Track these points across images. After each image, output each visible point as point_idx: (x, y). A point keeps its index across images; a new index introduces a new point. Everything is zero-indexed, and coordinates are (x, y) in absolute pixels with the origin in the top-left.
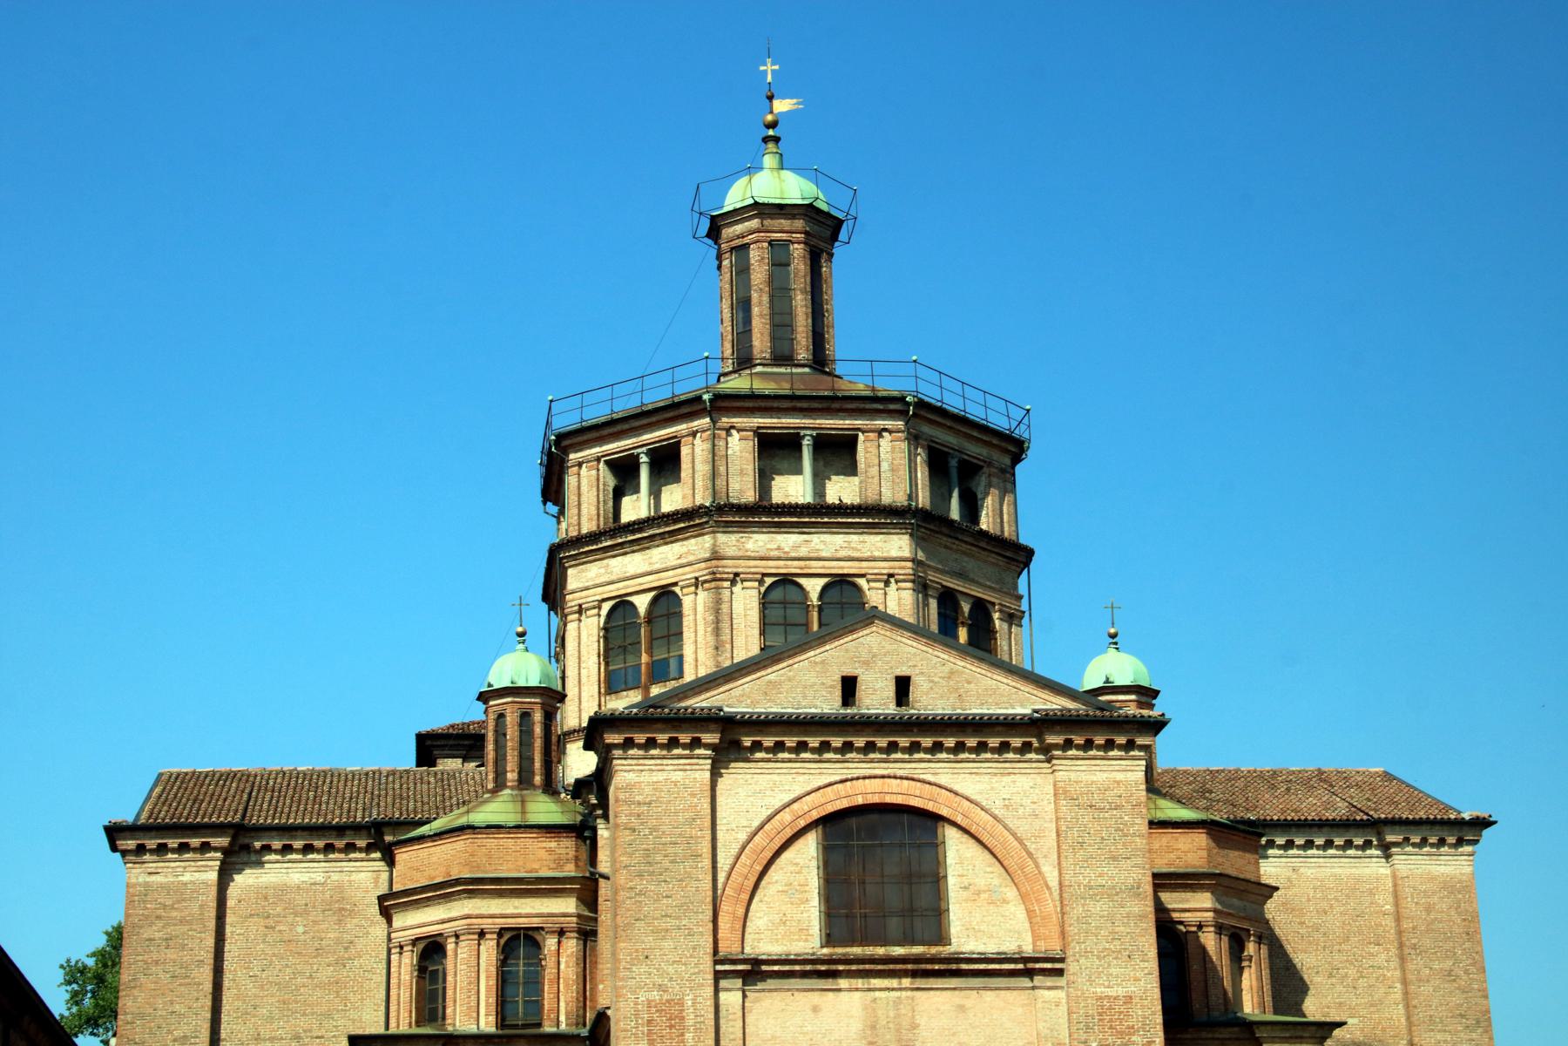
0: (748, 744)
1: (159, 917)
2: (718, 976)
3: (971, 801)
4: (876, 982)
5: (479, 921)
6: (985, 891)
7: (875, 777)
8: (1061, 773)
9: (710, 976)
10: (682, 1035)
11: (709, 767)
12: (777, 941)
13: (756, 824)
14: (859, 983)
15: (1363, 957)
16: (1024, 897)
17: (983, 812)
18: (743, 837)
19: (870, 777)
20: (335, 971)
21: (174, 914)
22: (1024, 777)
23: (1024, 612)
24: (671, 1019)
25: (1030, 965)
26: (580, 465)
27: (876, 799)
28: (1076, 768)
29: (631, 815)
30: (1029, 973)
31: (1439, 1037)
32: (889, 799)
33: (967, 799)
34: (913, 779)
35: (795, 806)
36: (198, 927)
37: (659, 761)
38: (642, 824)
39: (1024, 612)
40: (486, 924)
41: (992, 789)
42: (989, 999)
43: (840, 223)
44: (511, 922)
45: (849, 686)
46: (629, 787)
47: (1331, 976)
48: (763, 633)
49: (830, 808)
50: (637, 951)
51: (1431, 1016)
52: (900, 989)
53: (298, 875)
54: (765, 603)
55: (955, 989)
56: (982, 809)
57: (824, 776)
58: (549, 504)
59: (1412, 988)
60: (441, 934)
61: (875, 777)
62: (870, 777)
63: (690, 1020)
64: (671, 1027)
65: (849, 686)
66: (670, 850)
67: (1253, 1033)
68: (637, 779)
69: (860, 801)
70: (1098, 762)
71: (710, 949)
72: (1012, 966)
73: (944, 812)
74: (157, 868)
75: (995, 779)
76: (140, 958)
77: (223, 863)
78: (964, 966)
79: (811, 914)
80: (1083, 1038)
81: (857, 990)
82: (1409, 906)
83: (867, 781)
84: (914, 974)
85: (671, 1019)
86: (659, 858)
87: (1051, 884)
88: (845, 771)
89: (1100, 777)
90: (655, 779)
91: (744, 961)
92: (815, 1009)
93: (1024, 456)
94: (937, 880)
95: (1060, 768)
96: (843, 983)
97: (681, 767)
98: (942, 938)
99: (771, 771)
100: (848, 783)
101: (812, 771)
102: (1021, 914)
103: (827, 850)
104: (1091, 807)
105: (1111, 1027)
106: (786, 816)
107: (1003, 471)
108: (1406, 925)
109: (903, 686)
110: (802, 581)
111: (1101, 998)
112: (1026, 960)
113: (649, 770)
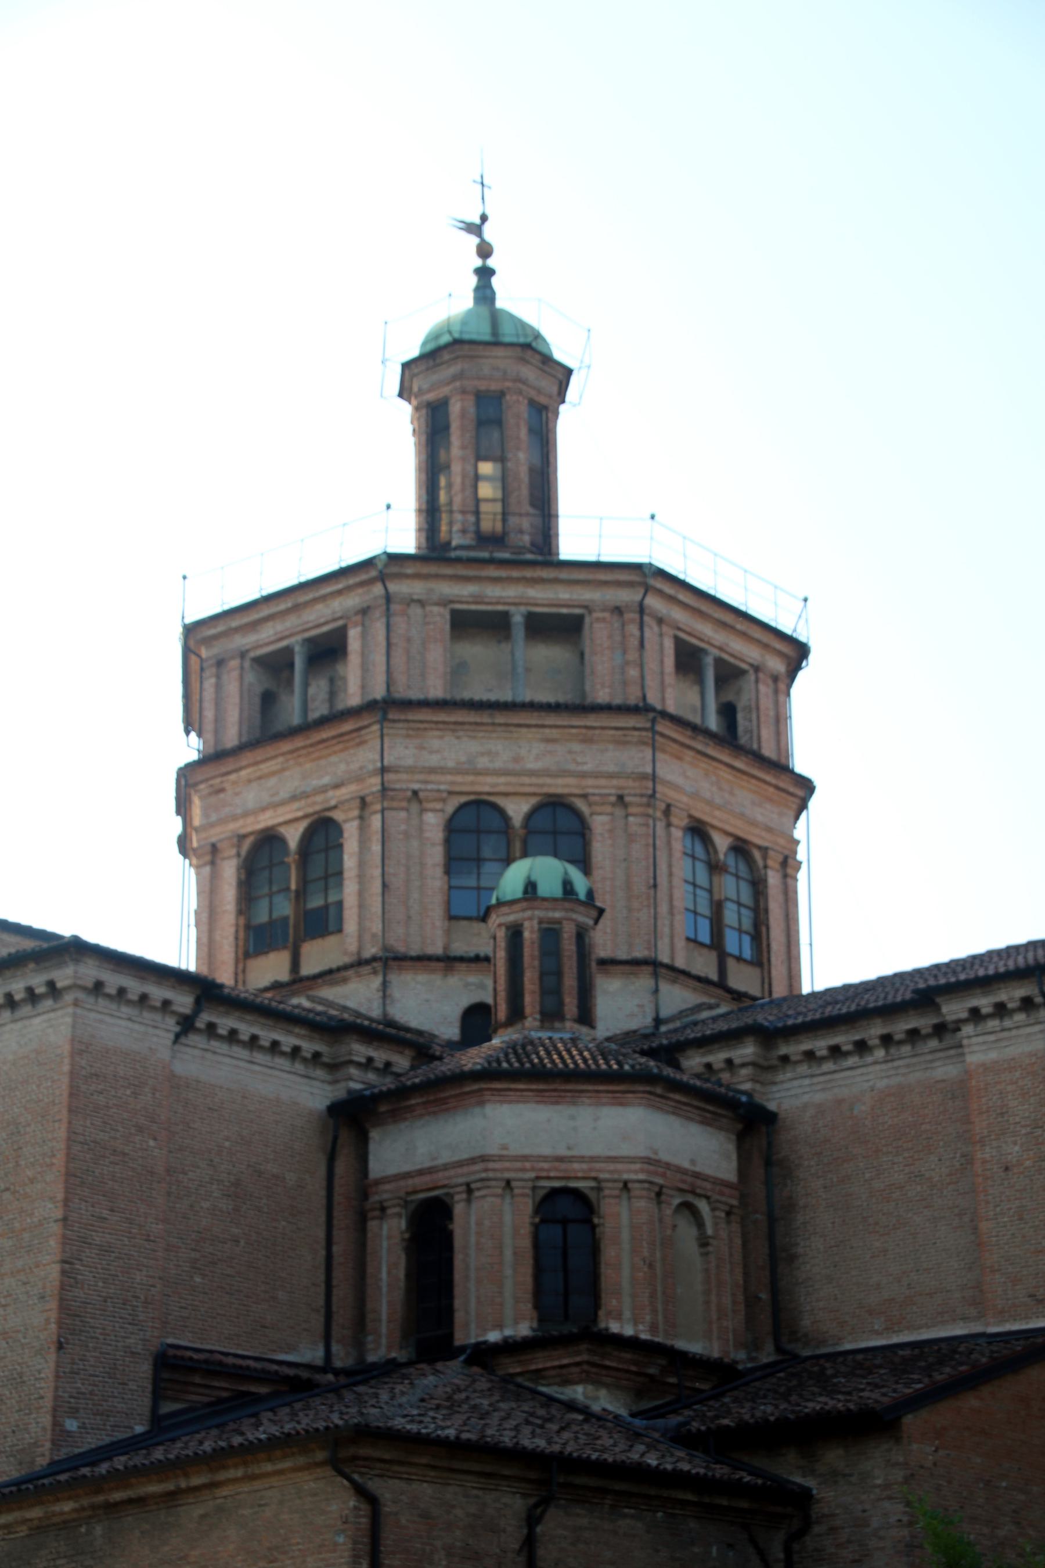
23: (800, 863)
39: (800, 863)
43: (569, 372)
48: (448, 871)
54: (452, 829)
58: (193, 735)
93: (804, 664)
107: (775, 679)
110: (500, 801)
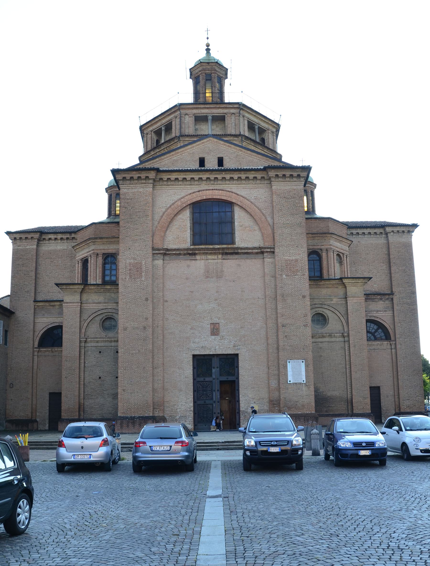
0: (166, 179)
1: (21, 258)
2: (153, 254)
3: (243, 197)
4: (209, 257)
5: (97, 251)
6: (248, 227)
7: (210, 190)
8: (274, 187)
9: (151, 255)
10: (141, 274)
11: (152, 186)
12: (175, 244)
13: (168, 206)
14: (203, 257)
15: (379, 267)
16: (260, 229)
17: (247, 201)
18: (164, 210)
19: (208, 190)
20: (70, 274)
21: (25, 257)
22: (262, 189)
24: (137, 269)
25: (263, 250)
26: (147, 134)
27: (210, 197)
28: (280, 185)
29: (125, 203)
30: (262, 253)
31: (401, 289)
32: (214, 197)
33: (242, 196)
34: (223, 190)
35: (182, 200)
36: (31, 261)
37: (135, 185)
38: (129, 206)
40: (99, 252)
41: (251, 193)
42: (248, 262)
44: (106, 252)
45: (202, 162)
46: (125, 194)
47: (369, 272)
49: (194, 200)
50: (126, 247)
51: (398, 283)
52: (218, 259)
53: (59, 247)
55: (237, 259)
56: (247, 200)
57: (192, 190)
59: (393, 275)
60: (87, 256)
61: (210, 190)
62: (208, 190)
63: (144, 269)
64: (137, 271)
65: (202, 162)
66: (138, 214)
67: (342, 281)
68: (127, 191)
69: (205, 198)
70: (287, 183)
71: (151, 245)
72: (257, 251)
73: (234, 201)
74: (20, 244)
75: (252, 190)
76: (16, 269)
77: (38, 243)
78: (240, 251)
79: (187, 235)
80: (280, 274)
81: (203, 259)
82: (392, 251)
83: (207, 191)
84: (222, 254)
85: (137, 269)
86: (134, 217)
87: (271, 224)
88: (199, 188)
89: (288, 188)
90: (133, 191)
91: (164, 249)
92: (188, 266)
94: (232, 222)
95: (274, 185)
96: (198, 257)
97: (142, 187)
98: (233, 243)
99: (174, 189)
100: (201, 192)
101: (188, 188)
102: (260, 235)
103: (193, 213)
104: (285, 197)
105: (290, 270)
106: (179, 203)
108: (391, 257)
109: (220, 161)
111: (287, 260)
112: (260, 248)
113: (132, 188)
